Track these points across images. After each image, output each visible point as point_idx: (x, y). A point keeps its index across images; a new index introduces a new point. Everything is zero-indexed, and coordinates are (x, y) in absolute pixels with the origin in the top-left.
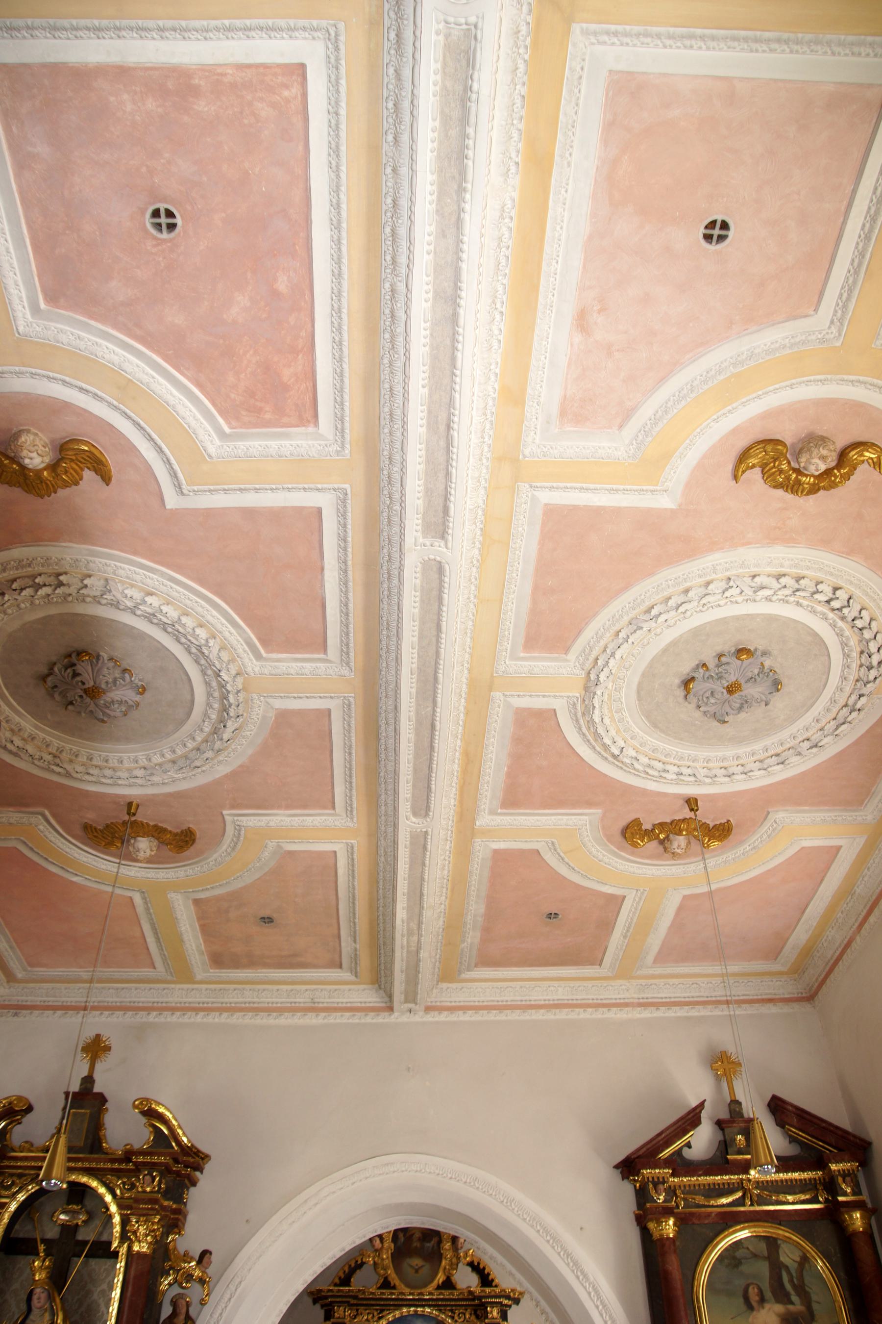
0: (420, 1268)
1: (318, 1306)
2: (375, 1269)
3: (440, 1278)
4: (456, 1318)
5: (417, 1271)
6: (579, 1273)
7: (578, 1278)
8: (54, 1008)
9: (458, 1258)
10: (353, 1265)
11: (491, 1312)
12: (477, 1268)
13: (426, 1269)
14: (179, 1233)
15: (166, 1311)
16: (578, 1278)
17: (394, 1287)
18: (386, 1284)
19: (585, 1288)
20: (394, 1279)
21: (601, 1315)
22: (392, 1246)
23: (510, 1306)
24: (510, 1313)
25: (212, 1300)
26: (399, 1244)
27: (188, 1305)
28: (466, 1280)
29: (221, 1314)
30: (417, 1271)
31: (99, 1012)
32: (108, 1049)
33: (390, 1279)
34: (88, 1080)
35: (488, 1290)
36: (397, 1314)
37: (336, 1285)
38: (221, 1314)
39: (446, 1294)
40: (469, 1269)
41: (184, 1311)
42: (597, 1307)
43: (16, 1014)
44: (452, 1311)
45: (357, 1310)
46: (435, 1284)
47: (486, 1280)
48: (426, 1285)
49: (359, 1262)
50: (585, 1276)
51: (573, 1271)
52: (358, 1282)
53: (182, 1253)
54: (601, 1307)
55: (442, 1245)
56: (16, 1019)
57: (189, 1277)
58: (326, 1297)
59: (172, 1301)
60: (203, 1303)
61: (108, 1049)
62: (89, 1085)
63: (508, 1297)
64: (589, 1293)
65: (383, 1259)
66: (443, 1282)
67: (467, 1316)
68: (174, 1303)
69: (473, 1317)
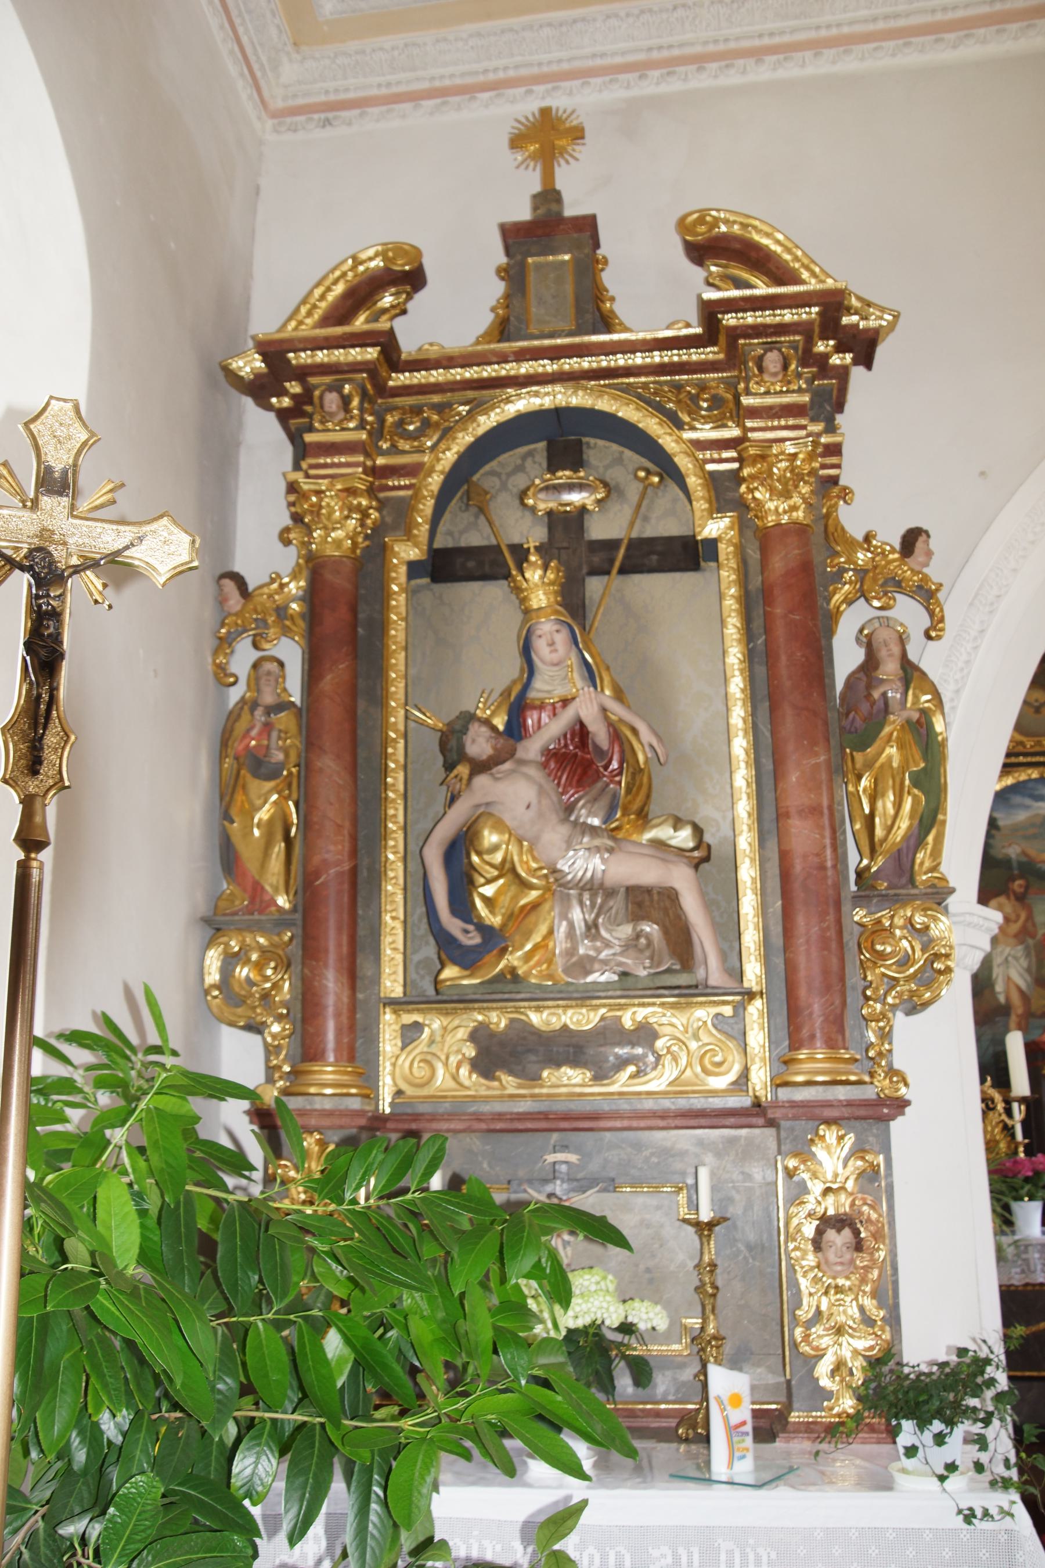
8: (414, 97)
27: (902, 640)
31: (522, 90)
32: (578, 134)
34: (549, 197)
41: (896, 650)
43: (327, 123)
53: (859, 537)
56: (328, 132)
61: (578, 134)
62: (554, 207)
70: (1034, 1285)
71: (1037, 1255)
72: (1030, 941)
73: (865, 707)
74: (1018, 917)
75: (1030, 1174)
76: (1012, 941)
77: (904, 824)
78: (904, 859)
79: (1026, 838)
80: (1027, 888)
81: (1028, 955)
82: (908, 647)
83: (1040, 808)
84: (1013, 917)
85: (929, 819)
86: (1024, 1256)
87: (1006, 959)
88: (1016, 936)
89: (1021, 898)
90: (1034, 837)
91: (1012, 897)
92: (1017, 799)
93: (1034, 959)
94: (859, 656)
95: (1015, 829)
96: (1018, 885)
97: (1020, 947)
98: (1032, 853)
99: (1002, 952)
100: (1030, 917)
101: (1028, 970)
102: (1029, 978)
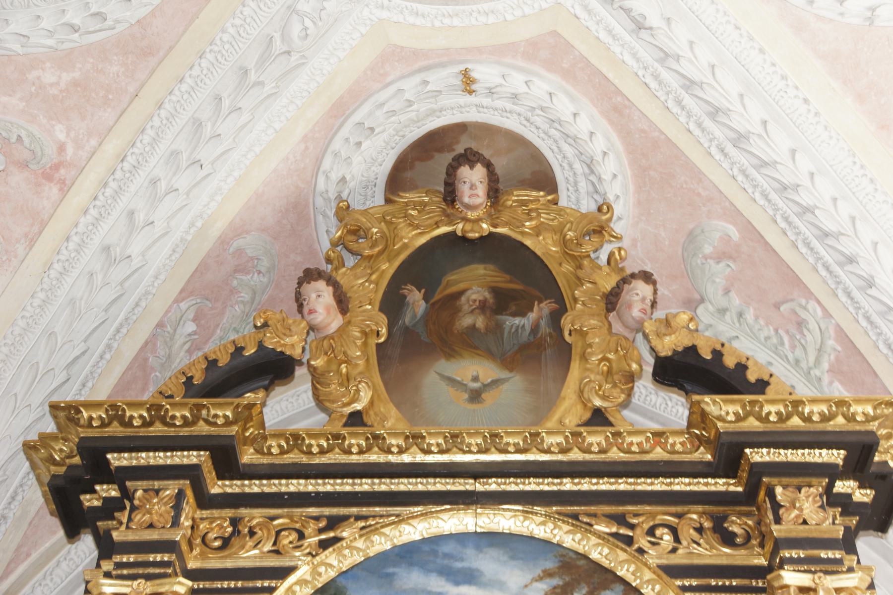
0: (486, 387)
4: (643, 542)
13: (513, 388)
26: (407, 319)
30: (476, 396)
44: (620, 520)
55: (566, 322)
67: (687, 533)
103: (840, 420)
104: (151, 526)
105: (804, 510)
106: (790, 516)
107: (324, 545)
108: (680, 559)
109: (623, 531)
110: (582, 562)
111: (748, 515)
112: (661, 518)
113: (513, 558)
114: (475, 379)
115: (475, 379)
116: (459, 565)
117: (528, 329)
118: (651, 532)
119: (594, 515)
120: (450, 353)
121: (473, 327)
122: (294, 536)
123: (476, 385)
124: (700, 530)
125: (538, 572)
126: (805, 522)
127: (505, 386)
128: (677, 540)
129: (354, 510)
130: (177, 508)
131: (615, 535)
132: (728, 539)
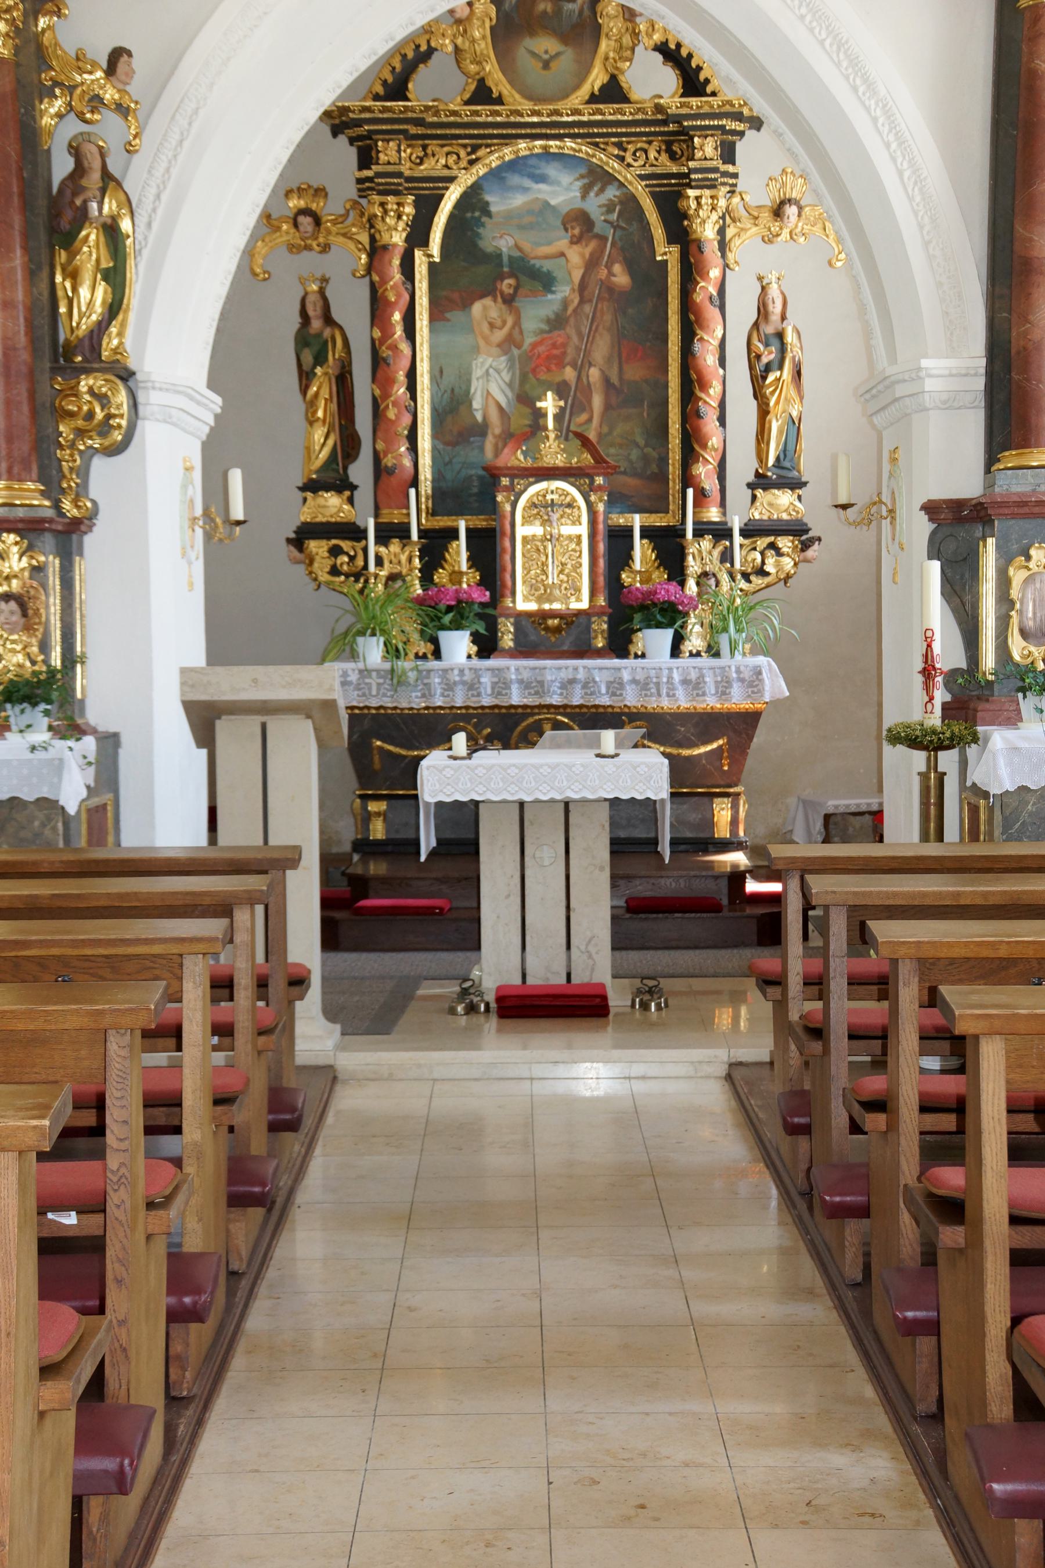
1: (343, 139)
2: (458, 62)
3: (597, 78)
4: (629, 159)
5: (546, 65)
6: (858, 81)
7: (855, 89)
9: (635, 35)
10: (410, 55)
11: (701, 149)
12: (672, 55)
13: (567, 59)
14: (59, 14)
15: (62, 166)
16: (855, 89)
17: (499, 101)
18: (482, 94)
19: (868, 109)
20: (498, 82)
21: (894, 159)
22: (493, 10)
23: (742, 134)
24: (740, 147)
25: (147, 144)
27: (102, 154)
28: (652, 82)
29: (168, 170)
30: (546, 65)
33: (490, 83)
35: (694, 101)
36: (508, 153)
37: (377, 97)
38: (168, 170)
39: (609, 112)
40: (659, 57)
41: (97, 164)
42: (888, 145)
44: (619, 146)
45: (424, 148)
46: (584, 92)
47: (693, 83)
48: (566, 96)
49: (424, 48)
50: (870, 85)
51: (847, 78)
52: (423, 91)
54: (894, 146)
57: (96, 102)
58: (359, 123)
59: (70, 146)
60: (130, 150)
63: (738, 117)
64: (875, 120)
65: (473, 41)
66: (602, 88)
67: (652, 154)
68: (75, 150)
69: (664, 157)
70: (435, 708)
71: (437, 680)
72: (516, 352)
73: (68, 214)
74: (504, 323)
75: (453, 603)
76: (495, 351)
77: (98, 308)
78: (95, 337)
79: (521, 227)
80: (517, 289)
81: (511, 368)
82: (108, 161)
83: (540, 191)
84: (499, 323)
85: (114, 309)
86: (426, 681)
87: (487, 372)
88: (499, 345)
89: (509, 301)
90: (531, 227)
91: (499, 299)
92: (515, 179)
93: (518, 372)
94: (70, 164)
95: (509, 216)
96: (507, 285)
97: (503, 358)
98: (527, 247)
99: (482, 363)
100: (517, 323)
101: (510, 385)
102: (510, 394)
103: (728, 106)
104: (389, 163)
105: (708, 148)
106: (698, 154)
107: (472, 163)
108: (649, 170)
109: (622, 153)
110: (599, 169)
111: (684, 141)
112: (639, 145)
113: (565, 167)
114: (546, 52)
115: (546, 52)
116: (538, 172)
117: (577, 12)
118: (634, 154)
119: (606, 144)
120: (532, 34)
121: (545, 12)
122: (455, 157)
123: (546, 57)
124: (659, 152)
125: (577, 175)
126: (706, 159)
127: (562, 57)
128: (647, 158)
129: (484, 141)
130: (399, 151)
131: (617, 156)
132: (673, 157)
